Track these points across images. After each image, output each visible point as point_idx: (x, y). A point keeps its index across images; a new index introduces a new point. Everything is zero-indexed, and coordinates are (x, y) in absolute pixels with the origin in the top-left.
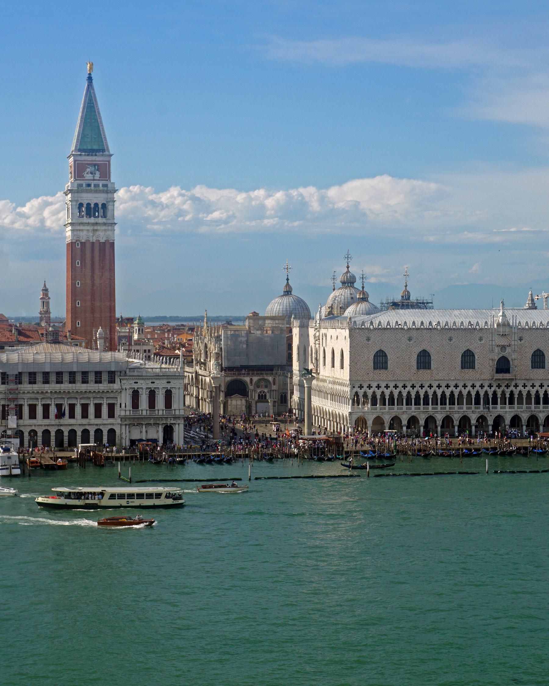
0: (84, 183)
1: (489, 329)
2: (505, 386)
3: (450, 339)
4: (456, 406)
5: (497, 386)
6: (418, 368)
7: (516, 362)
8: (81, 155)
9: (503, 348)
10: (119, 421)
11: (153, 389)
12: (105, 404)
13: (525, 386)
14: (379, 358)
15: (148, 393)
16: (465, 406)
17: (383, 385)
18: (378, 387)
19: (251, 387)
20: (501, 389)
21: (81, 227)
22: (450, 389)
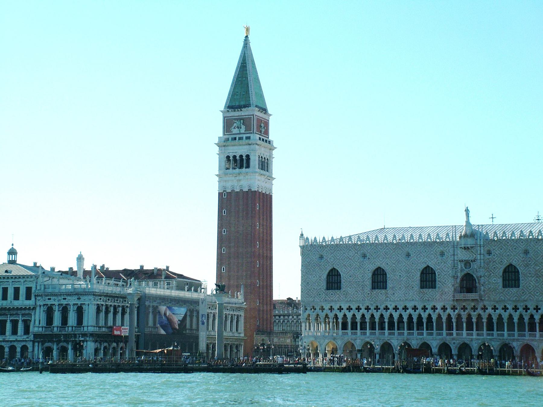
0: (230, 137)
1: (450, 242)
2: (472, 309)
4: (415, 332)
5: (462, 309)
6: (373, 288)
7: (482, 280)
9: (467, 263)
11: (64, 305)
12: (20, 320)
13: (495, 308)
14: (334, 277)
15: (61, 309)
17: (336, 307)
20: (467, 311)
21: (227, 178)
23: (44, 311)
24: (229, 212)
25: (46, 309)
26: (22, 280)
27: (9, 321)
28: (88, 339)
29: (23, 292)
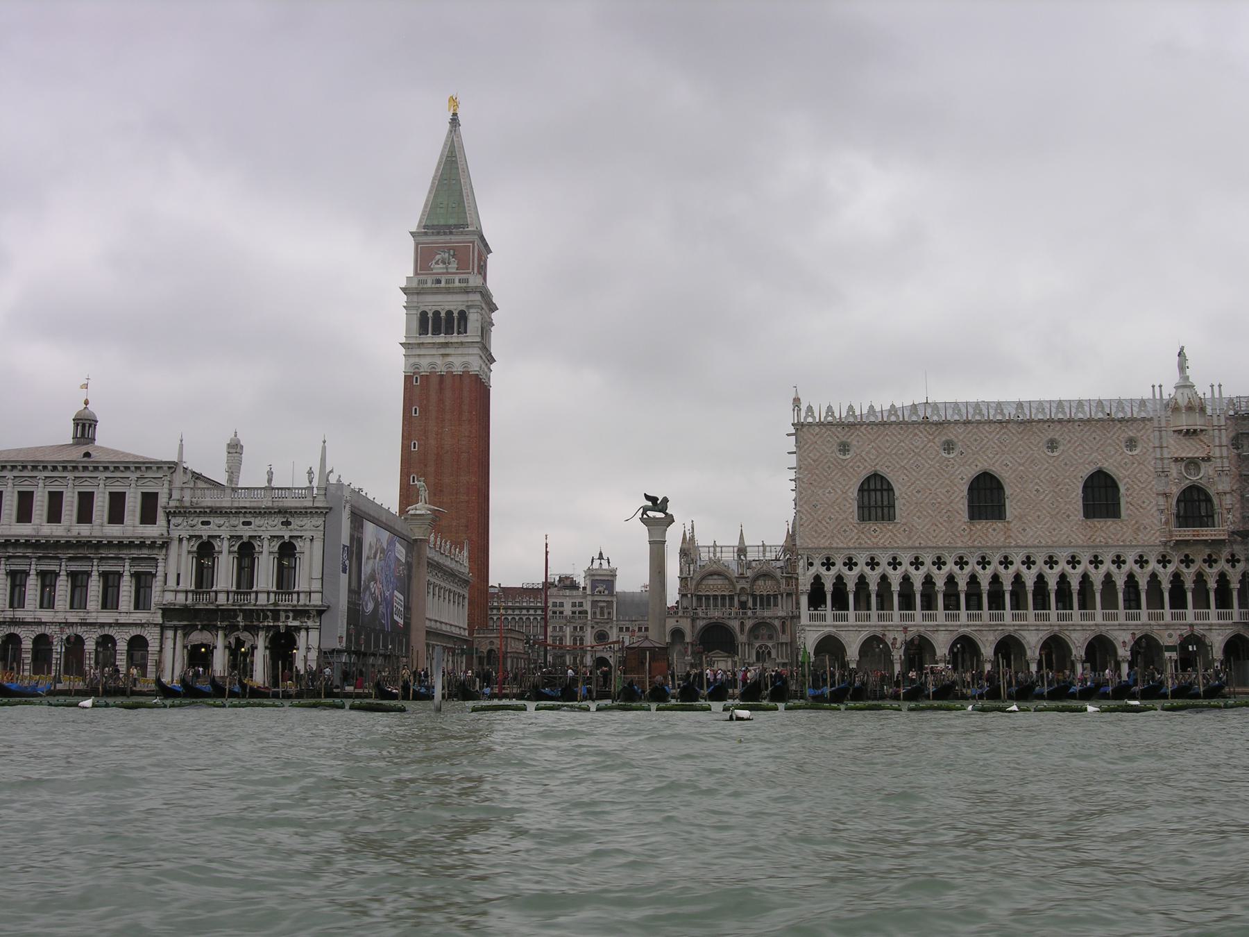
1: (1151, 419)
2: (1205, 561)
3: (1052, 445)
4: (1076, 612)
5: (1182, 562)
6: (972, 517)
8: (426, 234)
9: (1193, 463)
10: (159, 619)
11: (245, 540)
12: (127, 573)
14: (873, 494)
15: (236, 548)
16: (1099, 611)
17: (884, 559)
18: (873, 564)
19: (742, 638)
21: (422, 352)
22: (1057, 569)
23: (189, 552)
24: (424, 410)
25: (195, 549)
26: (133, 476)
27: (95, 574)
28: (310, 623)
29: (133, 505)
